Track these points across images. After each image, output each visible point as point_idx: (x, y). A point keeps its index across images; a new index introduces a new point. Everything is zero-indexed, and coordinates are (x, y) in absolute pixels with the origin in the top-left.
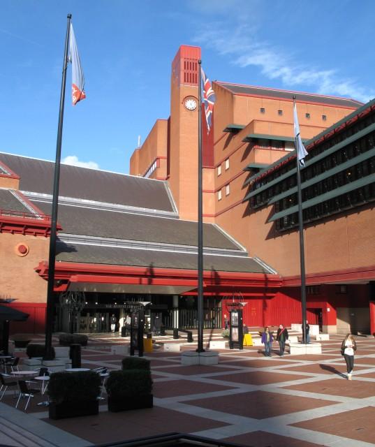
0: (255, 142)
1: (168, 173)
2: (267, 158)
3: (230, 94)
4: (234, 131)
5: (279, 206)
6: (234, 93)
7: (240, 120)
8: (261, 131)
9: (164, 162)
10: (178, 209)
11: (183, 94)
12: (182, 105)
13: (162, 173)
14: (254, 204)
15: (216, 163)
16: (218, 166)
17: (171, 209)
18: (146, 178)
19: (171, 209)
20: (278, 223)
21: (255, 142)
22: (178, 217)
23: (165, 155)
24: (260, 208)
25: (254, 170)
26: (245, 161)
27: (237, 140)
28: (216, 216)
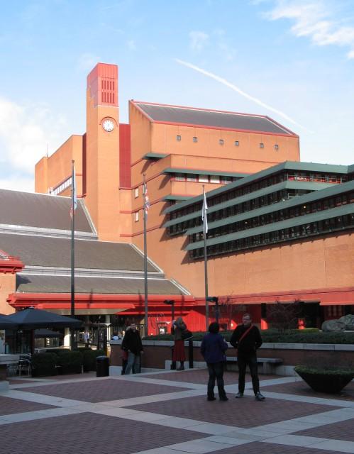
0: (172, 175)
1: (84, 191)
2: (184, 190)
3: (148, 122)
4: (153, 159)
5: (193, 239)
6: (153, 120)
7: (156, 150)
8: (177, 164)
9: (78, 181)
10: (97, 230)
11: (101, 114)
12: (99, 127)
13: (78, 190)
14: (172, 232)
15: (133, 185)
16: (135, 188)
17: (89, 230)
18: (54, 194)
19: (89, 230)
20: (192, 252)
21: (172, 175)
22: (97, 238)
23: (81, 172)
24: (176, 236)
25: (172, 202)
26: (162, 190)
27: (155, 168)
28: (133, 236)
